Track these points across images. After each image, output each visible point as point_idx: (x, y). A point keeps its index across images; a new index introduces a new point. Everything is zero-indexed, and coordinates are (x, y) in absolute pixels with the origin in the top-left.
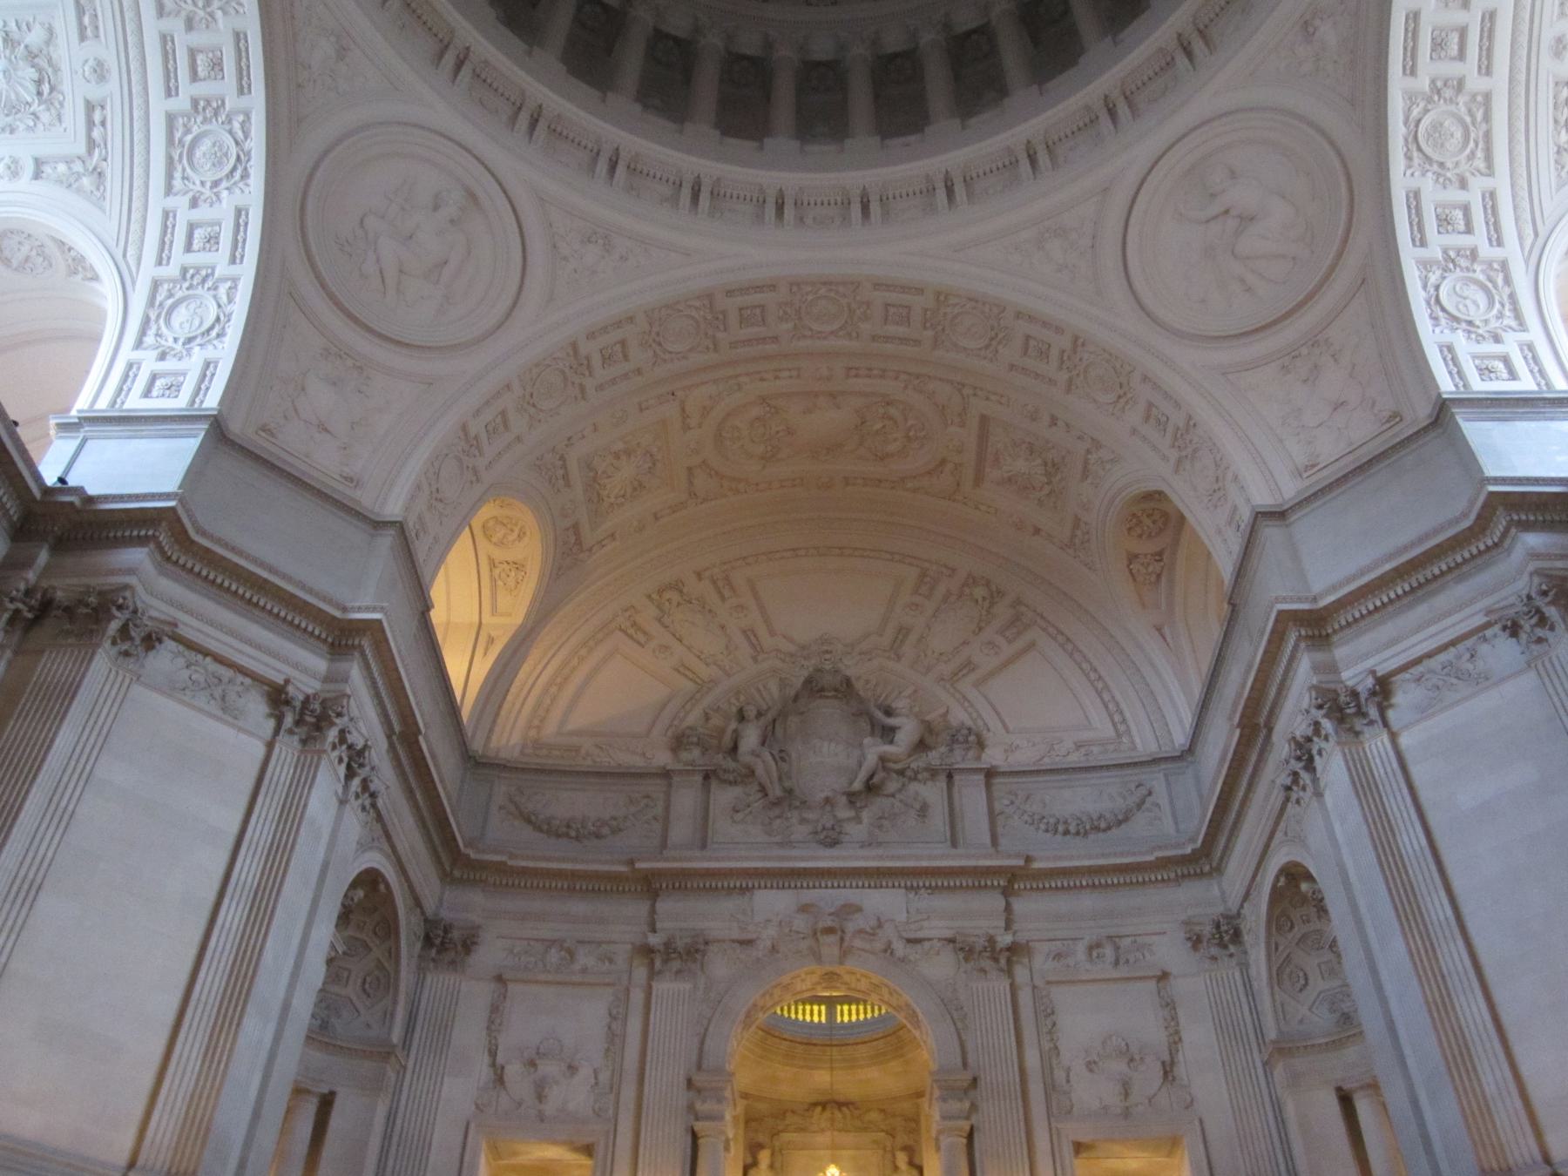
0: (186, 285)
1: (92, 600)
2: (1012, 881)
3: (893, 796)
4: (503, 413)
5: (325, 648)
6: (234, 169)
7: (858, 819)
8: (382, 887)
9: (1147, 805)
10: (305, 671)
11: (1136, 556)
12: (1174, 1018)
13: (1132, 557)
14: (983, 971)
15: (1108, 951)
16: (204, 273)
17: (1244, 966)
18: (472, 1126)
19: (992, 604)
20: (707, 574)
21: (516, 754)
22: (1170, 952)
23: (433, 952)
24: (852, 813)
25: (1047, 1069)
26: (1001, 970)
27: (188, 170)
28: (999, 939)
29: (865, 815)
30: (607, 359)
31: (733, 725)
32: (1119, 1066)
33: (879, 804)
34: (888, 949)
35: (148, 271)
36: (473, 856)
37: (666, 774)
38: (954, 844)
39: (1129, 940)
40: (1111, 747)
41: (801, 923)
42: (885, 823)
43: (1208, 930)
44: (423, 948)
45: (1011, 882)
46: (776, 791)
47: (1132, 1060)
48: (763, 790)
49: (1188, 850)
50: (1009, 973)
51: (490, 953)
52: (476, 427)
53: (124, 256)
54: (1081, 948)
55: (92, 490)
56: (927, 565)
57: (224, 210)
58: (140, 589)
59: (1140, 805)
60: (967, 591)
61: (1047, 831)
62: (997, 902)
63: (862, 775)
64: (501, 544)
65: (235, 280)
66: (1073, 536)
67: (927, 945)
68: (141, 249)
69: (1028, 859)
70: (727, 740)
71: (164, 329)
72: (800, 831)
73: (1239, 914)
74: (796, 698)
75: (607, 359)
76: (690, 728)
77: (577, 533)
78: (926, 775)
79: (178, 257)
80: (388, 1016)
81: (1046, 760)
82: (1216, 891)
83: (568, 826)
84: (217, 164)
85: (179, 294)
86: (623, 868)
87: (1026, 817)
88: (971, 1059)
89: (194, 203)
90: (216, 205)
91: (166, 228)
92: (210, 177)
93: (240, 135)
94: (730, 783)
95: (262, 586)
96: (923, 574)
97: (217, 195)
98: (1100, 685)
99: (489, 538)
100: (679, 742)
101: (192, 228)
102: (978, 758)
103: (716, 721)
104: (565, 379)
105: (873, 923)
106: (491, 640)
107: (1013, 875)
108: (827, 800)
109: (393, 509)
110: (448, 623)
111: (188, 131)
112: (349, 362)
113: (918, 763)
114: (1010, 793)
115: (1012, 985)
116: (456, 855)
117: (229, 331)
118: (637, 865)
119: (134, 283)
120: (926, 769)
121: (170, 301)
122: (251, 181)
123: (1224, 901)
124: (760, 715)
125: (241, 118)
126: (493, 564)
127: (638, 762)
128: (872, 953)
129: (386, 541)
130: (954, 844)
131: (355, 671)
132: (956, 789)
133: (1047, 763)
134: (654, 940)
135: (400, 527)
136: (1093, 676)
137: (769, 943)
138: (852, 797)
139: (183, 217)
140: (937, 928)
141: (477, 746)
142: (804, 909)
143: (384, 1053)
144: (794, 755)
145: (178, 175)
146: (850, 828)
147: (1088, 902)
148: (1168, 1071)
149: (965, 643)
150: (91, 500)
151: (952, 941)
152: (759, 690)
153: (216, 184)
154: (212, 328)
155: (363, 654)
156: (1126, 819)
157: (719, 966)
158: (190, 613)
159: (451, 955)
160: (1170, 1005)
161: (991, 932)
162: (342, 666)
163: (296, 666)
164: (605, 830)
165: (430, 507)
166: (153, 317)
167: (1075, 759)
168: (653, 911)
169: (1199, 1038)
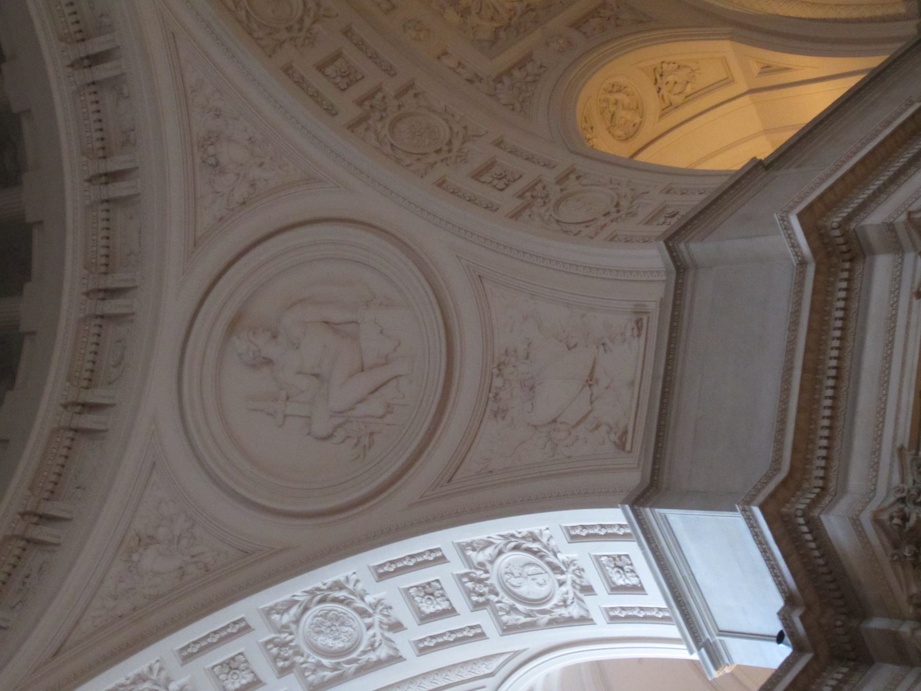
0: (493, 598)
1: (907, 551)
4: (476, 176)
5: (859, 268)
6: (336, 600)
10: (897, 280)
16: (470, 585)
27: (362, 648)
30: (350, 78)
35: (496, 643)
52: (508, 200)
53: (491, 675)
55: (778, 602)
57: (389, 592)
58: (873, 506)
64: (639, 108)
65: (462, 548)
68: (474, 662)
71: (555, 601)
75: (350, 78)
79: (466, 618)
84: (340, 620)
85: (508, 600)
89: (397, 626)
90: (387, 602)
91: (440, 644)
92: (360, 622)
93: (294, 610)
95: (812, 370)
97: (374, 606)
99: (637, 128)
101: (425, 618)
104: (399, 119)
106: (767, 69)
109: (654, 258)
110: (767, 131)
111: (319, 666)
112: (498, 382)
117: (525, 531)
119: (516, 653)
121: (520, 607)
122: (341, 577)
125: (276, 617)
126: (668, 109)
129: (697, 249)
131: (875, 219)
135: (671, 241)
139: (417, 632)
145: (373, 657)
150: (790, 600)
153: (363, 613)
154: (529, 550)
155: (849, 219)
158: (878, 438)
162: (873, 237)
163: (895, 292)
165: (633, 214)
166: (547, 618)
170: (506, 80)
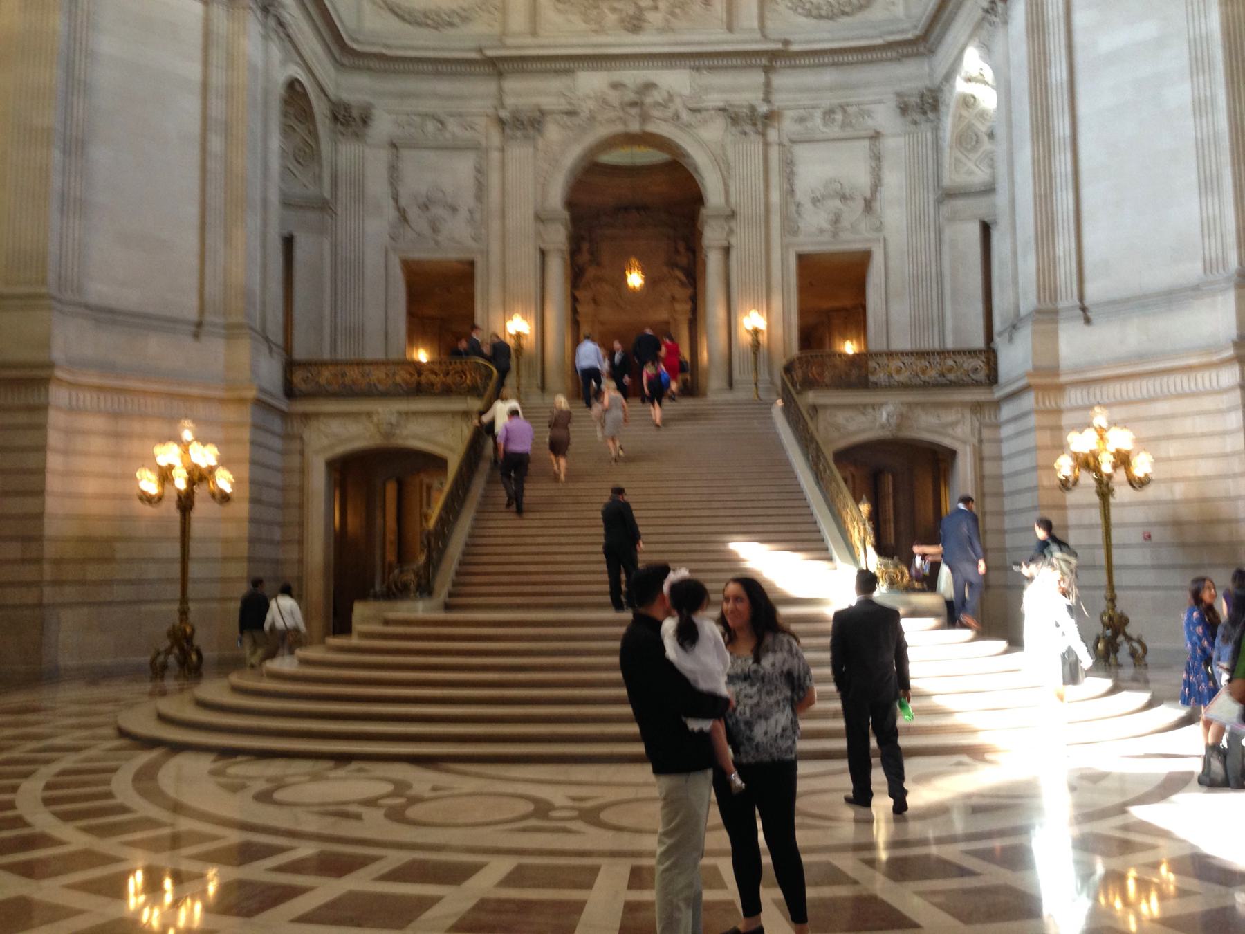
2: (774, 59)
14: (745, 133)
17: (936, 130)
22: (884, 117)
25: (785, 204)
26: (758, 132)
32: (836, 204)
34: (677, 117)
41: (614, 97)
43: (914, 100)
50: (764, 135)
51: (383, 125)
54: (818, 114)
62: (758, 78)
67: (705, 114)
69: (786, 42)
72: (611, 18)
82: (927, 69)
88: (733, 200)
105: (665, 95)
107: (773, 55)
123: (931, 76)
128: (665, 120)
140: (714, 100)
147: (828, 77)
151: (723, 110)
160: (877, 158)
164: (456, 20)
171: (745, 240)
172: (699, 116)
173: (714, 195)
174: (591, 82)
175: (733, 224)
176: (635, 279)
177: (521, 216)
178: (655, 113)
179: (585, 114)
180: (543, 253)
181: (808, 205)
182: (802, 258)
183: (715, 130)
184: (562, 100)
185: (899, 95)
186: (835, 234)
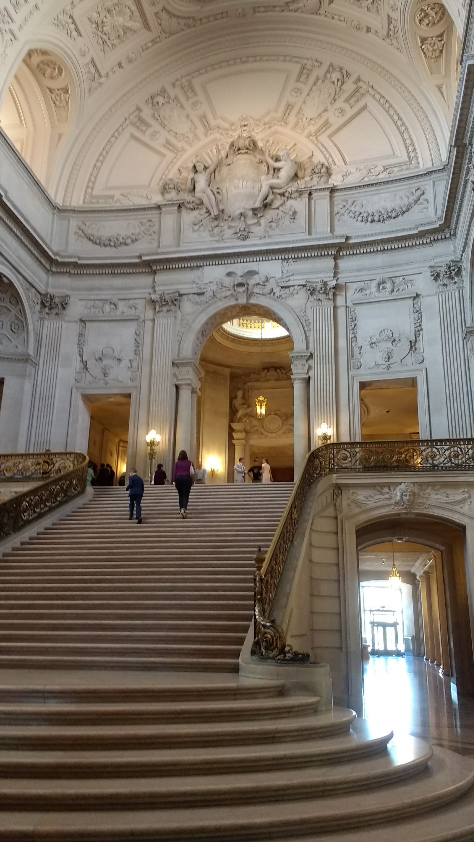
2: (340, 249)
3: (278, 208)
7: (259, 224)
8: (5, 280)
9: (421, 200)
11: (426, 39)
12: (420, 318)
13: (423, 40)
15: (389, 285)
17: (461, 289)
18: (74, 389)
19: (343, 83)
20: (178, 83)
21: (81, 203)
22: (423, 283)
23: (47, 310)
24: (256, 221)
25: (350, 348)
26: (329, 299)
28: (329, 283)
29: (263, 221)
31: (191, 175)
33: (270, 214)
36: (59, 260)
37: (159, 207)
38: (310, 233)
39: (401, 278)
40: (404, 167)
42: (274, 225)
43: (444, 269)
44: (41, 308)
45: (338, 251)
46: (215, 212)
47: (394, 341)
48: (208, 212)
49: (437, 226)
50: (334, 300)
51: (76, 308)
54: (374, 284)
56: (305, 61)
59: (416, 202)
60: (329, 76)
61: (362, 221)
62: (330, 263)
63: (260, 198)
66: (389, 30)
67: (292, 289)
69: (347, 238)
70: (189, 184)
72: (229, 233)
73: (461, 259)
74: (227, 157)
76: (171, 180)
77: (95, 65)
78: (296, 194)
80: (26, 341)
81: (366, 179)
82: (452, 248)
83: (110, 240)
86: (137, 260)
87: (351, 214)
88: (311, 345)
94: (192, 210)
96: (303, 68)
98: (403, 129)
100: (164, 190)
102: (327, 182)
103: (184, 174)
105: (264, 279)
107: (340, 247)
108: (241, 214)
113: (292, 187)
114: (344, 201)
115: (335, 308)
116: (52, 261)
118: (144, 258)
120: (297, 191)
124: (206, 168)
127: (143, 202)
130: (310, 233)
132: (313, 202)
133: (366, 181)
134: (154, 297)
136: (399, 123)
137: (211, 293)
138: (255, 211)
140: (298, 280)
141: (59, 201)
142: (229, 274)
143: (26, 359)
144: (224, 191)
146: (254, 229)
147: (379, 259)
148: (413, 346)
149: (326, 110)
151: (304, 286)
152: (208, 154)
156: (408, 210)
157: (187, 306)
159: (54, 311)
160: (419, 312)
161: (325, 280)
164: (129, 241)
167: (383, 177)
168: (154, 281)
169: (432, 327)
170: (70, 21)
171: (321, 374)
172: (287, 290)
173: (299, 345)
174: (214, 274)
175: (311, 362)
176: (261, 410)
177: (163, 362)
178: (256, 290)
179: (209, 294)
180: (177, 387)
181: (366, 347)
182: (363, 385)
183: (299, 299)
184: (194, 286)
185: (431, 267)
186: (388, 367)
